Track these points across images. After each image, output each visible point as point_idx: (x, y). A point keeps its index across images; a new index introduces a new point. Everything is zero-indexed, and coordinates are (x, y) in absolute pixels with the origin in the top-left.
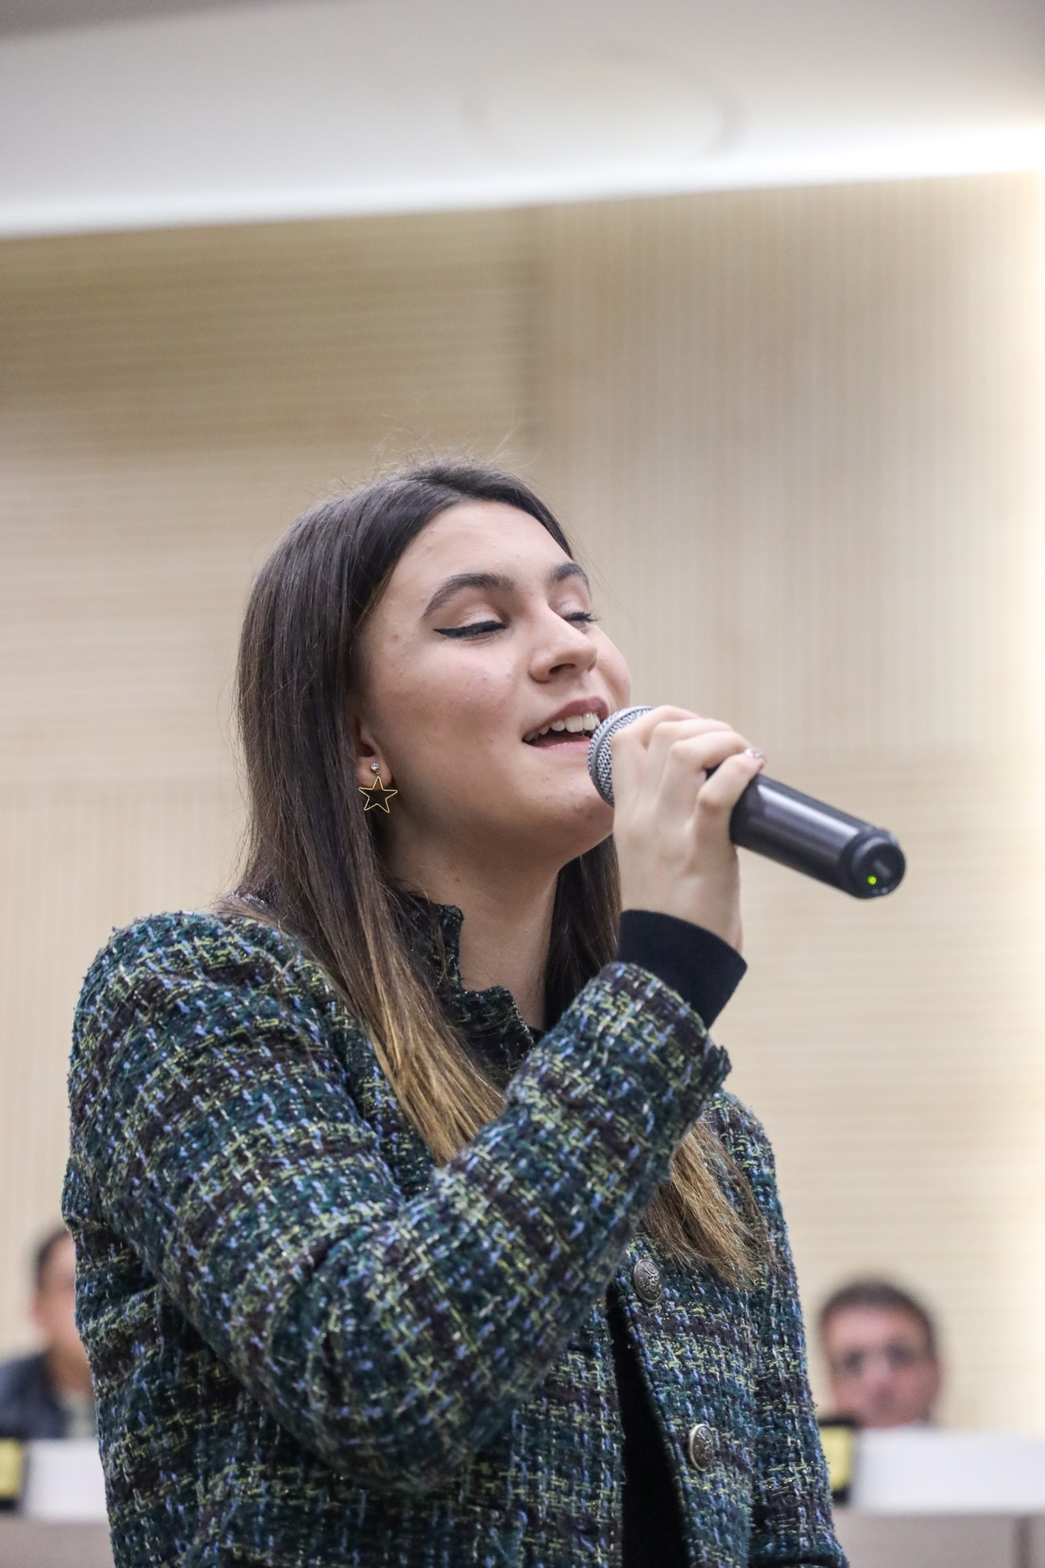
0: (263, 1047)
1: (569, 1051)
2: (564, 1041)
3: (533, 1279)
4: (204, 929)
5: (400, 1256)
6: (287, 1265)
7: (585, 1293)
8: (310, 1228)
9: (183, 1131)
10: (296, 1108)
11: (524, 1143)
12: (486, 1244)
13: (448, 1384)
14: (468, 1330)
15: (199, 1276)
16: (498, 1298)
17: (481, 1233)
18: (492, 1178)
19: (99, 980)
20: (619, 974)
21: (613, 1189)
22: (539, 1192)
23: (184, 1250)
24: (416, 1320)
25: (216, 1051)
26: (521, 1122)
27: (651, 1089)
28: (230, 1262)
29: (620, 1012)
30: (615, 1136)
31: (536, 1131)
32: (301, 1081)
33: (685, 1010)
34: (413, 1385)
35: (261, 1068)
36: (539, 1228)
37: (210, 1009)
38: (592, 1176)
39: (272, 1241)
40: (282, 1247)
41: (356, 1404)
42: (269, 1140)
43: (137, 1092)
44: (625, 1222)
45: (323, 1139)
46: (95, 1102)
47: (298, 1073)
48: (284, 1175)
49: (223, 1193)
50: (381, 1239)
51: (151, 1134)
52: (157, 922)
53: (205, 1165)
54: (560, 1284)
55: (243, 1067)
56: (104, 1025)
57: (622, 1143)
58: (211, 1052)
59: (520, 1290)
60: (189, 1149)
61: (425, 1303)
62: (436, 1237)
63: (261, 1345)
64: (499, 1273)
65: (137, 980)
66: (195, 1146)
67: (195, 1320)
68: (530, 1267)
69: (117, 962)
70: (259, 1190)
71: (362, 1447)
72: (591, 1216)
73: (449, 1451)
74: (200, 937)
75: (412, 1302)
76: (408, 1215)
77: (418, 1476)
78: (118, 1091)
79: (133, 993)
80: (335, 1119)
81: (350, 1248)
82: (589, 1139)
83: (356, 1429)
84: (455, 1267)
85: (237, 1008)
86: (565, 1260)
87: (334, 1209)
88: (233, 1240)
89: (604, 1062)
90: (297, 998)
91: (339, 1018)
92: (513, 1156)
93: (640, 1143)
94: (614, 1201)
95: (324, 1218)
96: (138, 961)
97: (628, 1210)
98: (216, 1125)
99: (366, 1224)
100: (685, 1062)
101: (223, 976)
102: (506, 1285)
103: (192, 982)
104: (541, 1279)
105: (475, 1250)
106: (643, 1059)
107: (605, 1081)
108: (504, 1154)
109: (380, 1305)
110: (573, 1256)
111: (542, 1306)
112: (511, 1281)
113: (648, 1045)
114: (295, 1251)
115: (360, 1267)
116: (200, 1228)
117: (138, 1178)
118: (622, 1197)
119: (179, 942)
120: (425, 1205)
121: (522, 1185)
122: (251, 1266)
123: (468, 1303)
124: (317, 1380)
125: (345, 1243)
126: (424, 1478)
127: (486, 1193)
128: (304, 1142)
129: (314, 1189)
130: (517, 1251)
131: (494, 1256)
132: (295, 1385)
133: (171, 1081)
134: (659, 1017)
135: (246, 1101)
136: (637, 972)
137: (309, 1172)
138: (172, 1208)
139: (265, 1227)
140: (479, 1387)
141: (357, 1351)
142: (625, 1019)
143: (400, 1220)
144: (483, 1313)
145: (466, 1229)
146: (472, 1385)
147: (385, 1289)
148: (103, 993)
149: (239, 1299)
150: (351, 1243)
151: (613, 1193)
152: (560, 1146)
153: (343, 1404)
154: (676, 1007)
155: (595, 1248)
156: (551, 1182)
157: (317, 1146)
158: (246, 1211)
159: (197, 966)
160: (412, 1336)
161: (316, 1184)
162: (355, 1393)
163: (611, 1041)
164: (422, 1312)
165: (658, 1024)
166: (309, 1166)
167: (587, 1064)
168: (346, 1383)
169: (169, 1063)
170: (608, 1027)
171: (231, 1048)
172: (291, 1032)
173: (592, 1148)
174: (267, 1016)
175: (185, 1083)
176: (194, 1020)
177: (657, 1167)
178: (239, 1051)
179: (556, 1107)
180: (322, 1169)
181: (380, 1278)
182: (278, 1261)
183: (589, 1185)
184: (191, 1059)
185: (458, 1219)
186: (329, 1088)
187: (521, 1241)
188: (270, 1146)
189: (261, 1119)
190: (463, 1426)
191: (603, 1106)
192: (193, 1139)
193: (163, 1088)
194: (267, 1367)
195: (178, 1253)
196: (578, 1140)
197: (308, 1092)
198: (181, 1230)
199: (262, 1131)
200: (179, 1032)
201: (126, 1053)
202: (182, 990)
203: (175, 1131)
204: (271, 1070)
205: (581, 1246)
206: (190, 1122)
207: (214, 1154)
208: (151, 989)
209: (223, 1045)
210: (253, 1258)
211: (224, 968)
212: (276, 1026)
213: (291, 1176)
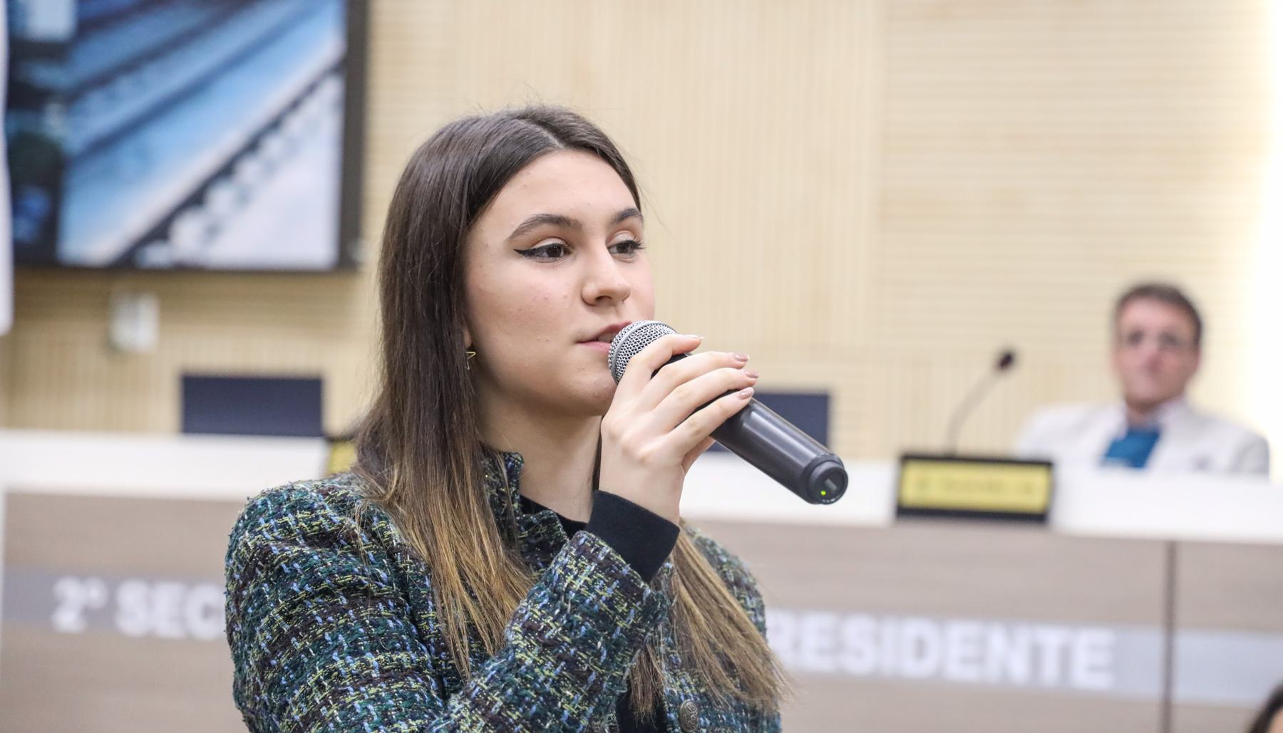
0: (342, 597)
1: (546, 601)
2: (542, 593)
4: (305, 503)
10: (363, 644)
11: (511, 676)
18: (488, 703)
20: (582, 541)
21: (577, 706)
25: (307, 602)
26: (510, 658)
31: (519, 666)
32: (367, 621)
33: (627, 570)
35: (338, 614)
38: (561, 698)
42: (340, 672)
45: (381, 669)
47: (366, 616)
48: (348, 700)
49: (308, 713)
53: (296, 692)
55: (325, 614)
56: (237, 576)
57: (583, 672)
58: (305, 604)
65: (255, 545)
70: (331, 712)
74: (300, 510)
80: (394, 650)
82: (558, 669)
87: (381, 727)
89: (569, 611)
90: (370, 553)
91: (402, 566)
92: (503, 685)
93: (597, 670)
94: (579, 715)
96: (257, 530)
97: (590, 720)
98: (306, 660)
100: (627, 608)
101: (317, 541)
107: (570, 624)
108: (498, 684)
113: (599, 597)
118: (584, 711)
119: (286, 515)
127: (483, 715)
129: (369, 710)
134: (608, 575)
135: (327, 641)
136: (594, 540)
137: (367, 697)
138: (278, 722)
142: (583, 577)
152: (536, 677)
156: (530, 705)
157: (374, 675)
159: (299, 534)
165: (607, 581)
167: (557, 611)
170: (571, 584)
171: (318, 599)
173: (561, 676)
174: (344, 574)
175: (286, 628)
176: (292, 579)
177: (612, 686)
179: (534, 646)
180: (377, 694)
183: (559, 704)
184: (290, 609)
186: (391, 624)
188: (340, 677)
189: (335, 656)
191: (569, 644)
193: (271, 631)
196: (550, 671)
197: (373, 630)
199: (335, 665)
202: (284, 555)
203: (279, 664)
204: (346, 615)
206: (288, 658)
207: (302, 684)
208: (264, 552)
209: (313, 597)
211: (318, 535)
212: (350, 581)
213: (354, 700)
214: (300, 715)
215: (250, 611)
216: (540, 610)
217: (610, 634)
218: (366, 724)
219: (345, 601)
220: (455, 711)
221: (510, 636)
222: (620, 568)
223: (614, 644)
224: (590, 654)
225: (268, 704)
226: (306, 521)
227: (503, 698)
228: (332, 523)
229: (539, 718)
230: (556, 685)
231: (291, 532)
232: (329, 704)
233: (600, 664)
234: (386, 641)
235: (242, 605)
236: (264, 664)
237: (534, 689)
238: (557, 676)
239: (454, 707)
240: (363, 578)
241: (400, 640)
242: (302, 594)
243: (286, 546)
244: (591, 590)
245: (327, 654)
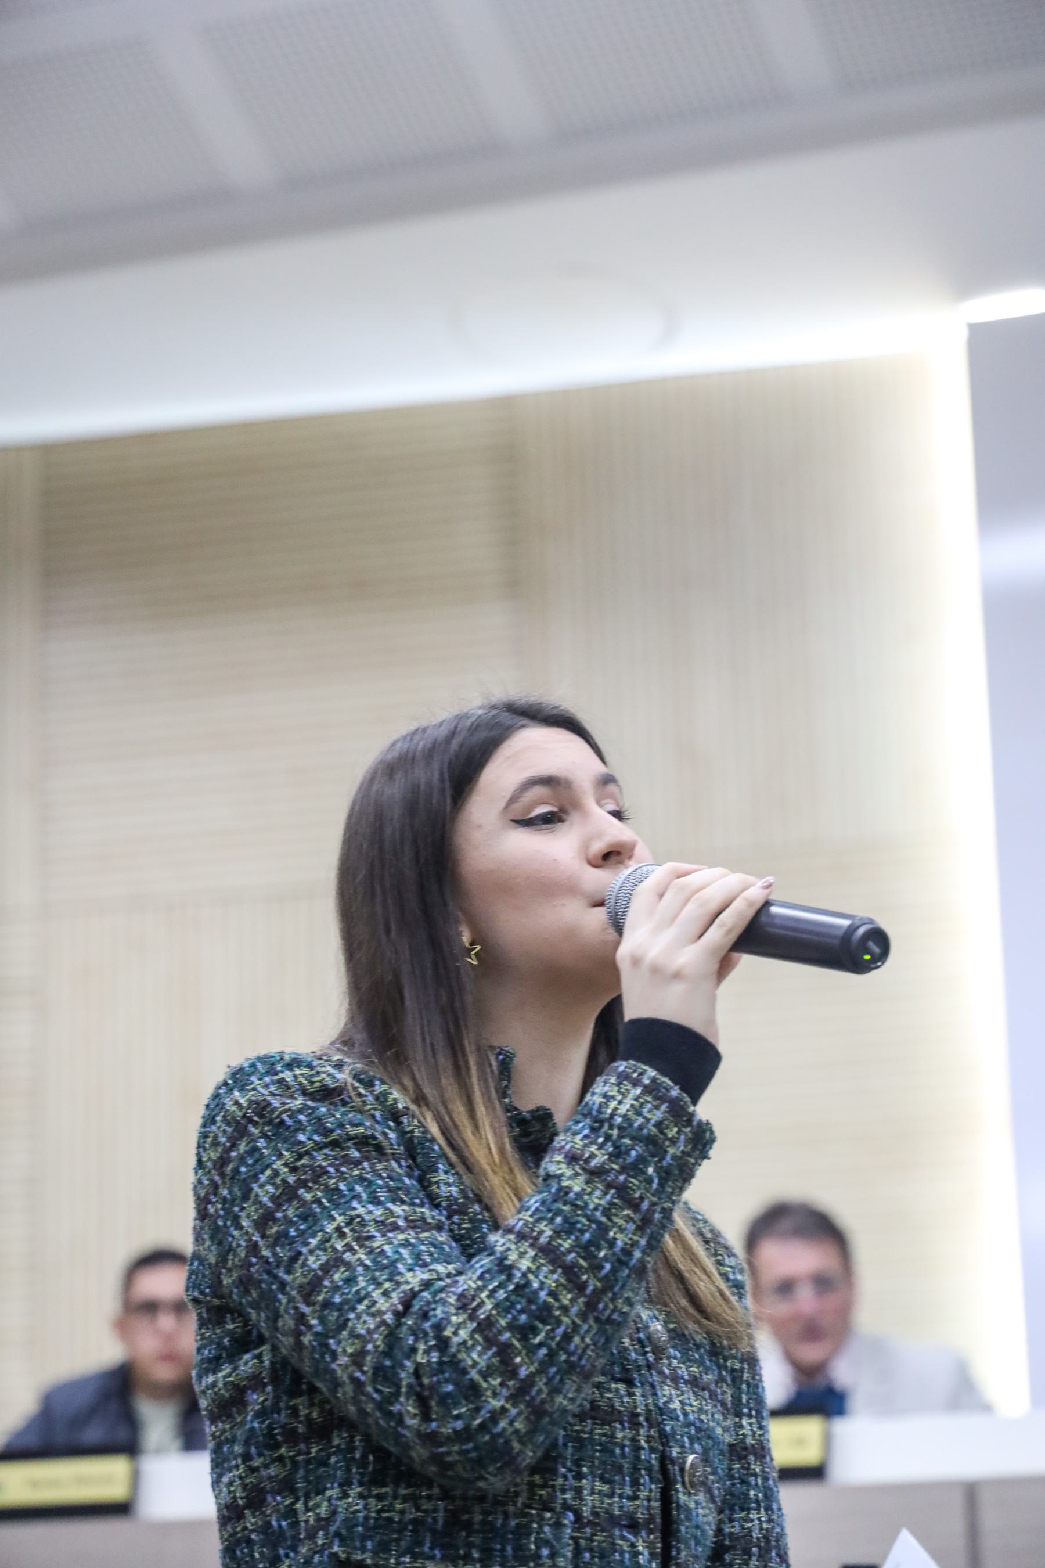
3: (574, 1310)
6: (380, 1313)
7: (614, 1320)
9: (291, 1216)
11: (559, 1205)
12: (536, 1285)
13: (514, 1398)
14: (527, 1355)
15: (310, 1327)
16: (549, 1327)
17: (531, 1276)
19: (217, 1105)
21: (630, 1236)
22: (574, 1241)
23: (296, 1308)
25: (315, 1153)
28: (336, 1314)
30: (630, 1194)
31: (567, 1193)
34: (486, 1401)
36: (576, 1269)
38: (613, 1227)
39: (368, 1295)
40: (376, 1299)
41: (442, 1419)
43: (252, 1189)
44: (642, 1263)
46: (217, 1201)
48: (376, 1244)
49: (328, 1261)
50: (452, 1289)
51: (265, 1220)
52: (262, 1059)
53: (311, 1240)
54: (595, 1314)
55: (337, 1165)
56: (223, 1140)
57: (635, 1199)
58: (312, 1155)
59: (565, 1319)
60: (297, 1230)
61: (491, 1335)
62: (496, 1284)
63: (363, 1378)
64: (547, 1307)
65: (250, 1101)
66: (302, 1227)
67: (307, 1367)
68: (571, 1300)
69: (232, 1090)
70: (357, 1257)
71: (449, 1453)
72: (615, 1258)
73: (518, 1454)
75: (480, 1336)
76: (473, 1270)
77: (495, 1475)
78: (236, 1189)
81: (429, 1297)
82: (608, 1197)
83: (443, 1440)
84: (513, 1305)
85: (331, 1120)
86: (598, 1294)
87: (417, 1268)
92: (550, 1215)
94: (632, 1245)
95: (409, 1275)
97: (643, 1252)
98: (318, 1210)
99: (441, 1279)
103: (294, 1101)
104: (580, 1310)
105: (527, 1290)
108: (543, 1215)
109: (456, 1340)
111: (582, 1332)
112: (557, 1313)
114: (386, 1301)
117: (255, 1257)
118: (637, 1242)
119: (282, 1072)
120: (486, 1261)
121: (559, 1237)
122: (352, 1316)
123: (525, 1332)
124: (411, 1402)
125: (425, 1294)
126: (500, 1477)
127: (532, 1245)
130: (561, 1288)
131: (543, 1294)
132: (392, 1408)
139: (362, 1284)
140: (538, 1400)
143: (467, 1275)
144: (537, 1340)
145: (518, 1275)
146: (533, 1399)
147: (459, 1326)
148: (222, 1114)
149: (344, 1343)
150: (430, 1294)
151: (631, 1239)
152: (586, 1204)
155: (620, 1284)
156: (582, 1232)
158: (347, 1273)
159: (298, 1090)
160: (482, 1363)
161: (402, 1251)
164: (489, 1342)
168: (433, 1403)
169: (278, 1165)
171: (326, 1151)
173: (611, 1204)
175: (291, 1179)
176: (297, 1130)
177: (663, 1218)
178: (333, 1153)
182: (373, 1309)
183: (611, 1234)
185: (511, 1267)
187: (563, 1281)
188: (363, 1223)
190: (527, 1432)
192: (300, 1222)
193: (273, 1184)
194: (368, 1395)
195: (292, 1312)
198: (294, 1293)
200: (285, 1140)
201: (242, 1159)
205: (609, 1283)
207: (319, 1232)
208: (262, 1108)
209: (321, 1149)
210: (353, 1309)
214: (319, 1262)
218: (400, 1266)
219: (357, 1154)
220: (499, 1244)
224: (640, 1179)
227: (550, 1226)
229: (593, 1245)
230: (607, 1212)
231: (289, 1088)
233: (652, 1191)
237: (586, 1216)
239: (497, 1241)
242: (310, 1144)
245: (345, 1203)
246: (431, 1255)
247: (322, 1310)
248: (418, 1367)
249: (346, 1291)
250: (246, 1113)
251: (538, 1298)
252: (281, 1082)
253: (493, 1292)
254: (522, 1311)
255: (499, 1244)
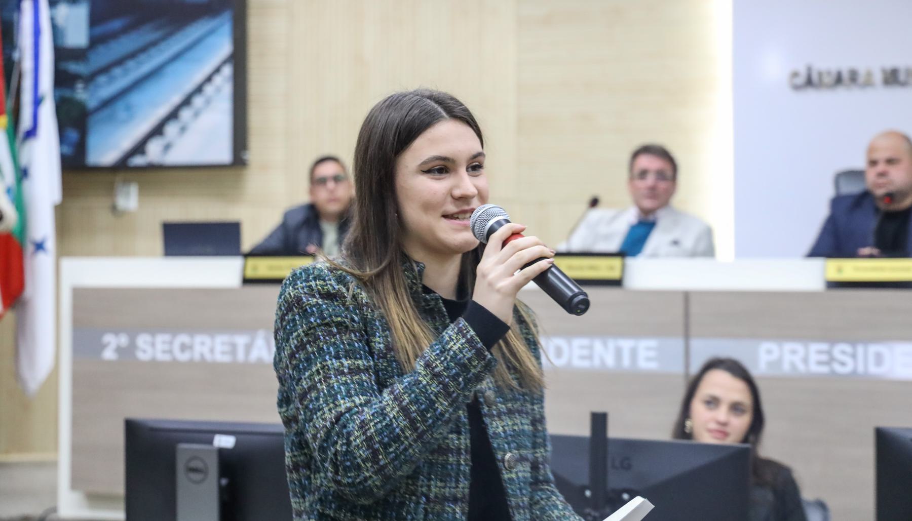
0: (335, 328)
1: (438, 352)
3: (410, 439)
4: (322, 276)
5: (364, 425)
8: (336, 406)
11: (415, 388)
12: (395, 425)
17: (394, 420)
20: (461, 325)
24: (367, 450)
25: (317, 328)
27: (463, 372)
29: (457, 342)
30: (448, 389)
31: (419, 384)
32: (345, 342)
33: (480, 345)
37: (317, 312)
39: (322, 409)
42: (329, 367)
48: (331, 382)
49: (311, 385)
50: (360, 416)
58: (315, 329)
59: (406, 442)
60: (303, 366)
64: (398, 436)
65: (294, 295)
70: (322, 387)
74: (319, 280)
79: (293, 301)
80: (356, 358)
82: (438, 388)
84: (383, 432)
86: (424, 432)
88: (311, 405)
90: (351, 306)
92: (410, 392)
94: (445, 412)
95: (342, 402)
96: (296, 287)
97: (450, 415)
98: (313, 357)
99: (357, 407)
102: (401, 441)
106: (462, 361)
108: (407, 390)
109: (354, 443)
110: (427, 431)
112: (402, 439)
113: (464, 356)
115: (351, 426)
116: (303, 397)
119: (311, 281)
122: (315, 417)
123: (386, 446)
125: (347, 415)
127: (398, 405)
128: (342, 368)
129: (340, 388)
133: (300, 337)
134: (470, 346)
137: (340, 381)
139: (321, 402)
141: (346, 458)
142: (458, 345)
144: (391, 450)
147: (357, 437)
152: (427, 390)
153: (338, 475)
154: (477, 343)
156: (421, 404)
157: (346, 371)
161: (342, 387)
162: (343, 473)
163: (452, 353)
164: (369, 447)
166: (341, 379)
167: (443, 359)
170: (452, 347)
172: (345, 322)
173: (439, 392)
174: (337, 316)
175: (305, 339)
176: (311, 315)
180: (346, 381)
181: (356, 432)
183: (436, 405)
188: (329, 369)
189: (327, 357)
193: (297, 340)
203: (299, 357)
204: (335, 337)
208: (299, 300)
210: (316, 414)
213: (334, 383)
215: (288, 327)
216: (434, 356)
217: (467, 375)
218: (339, 396)
221: (418, 367)
222: (477, 344)
223: (468, 380)
225: (292, 375)
226: (322, 286)
228: (334, 289)
230: (436, 395)
231: (313, 290)
232: (322, 382)
234: (353, 354)
235: (284, 323)
236: (292, 356)
238: (438, 391)
240: (346, 320)
241: (360, 354)
242: (315, 324)
243: (310, 297)
244: (461, 352)
246: (356, 390)
247: (305, 409)
248: (337, 451)
249: (315, 403)
250: (293, 301)
251: (395, 432)
252: (310, 286)
253: (376, 424)
254: (386, 436)
255: (385, 400)
